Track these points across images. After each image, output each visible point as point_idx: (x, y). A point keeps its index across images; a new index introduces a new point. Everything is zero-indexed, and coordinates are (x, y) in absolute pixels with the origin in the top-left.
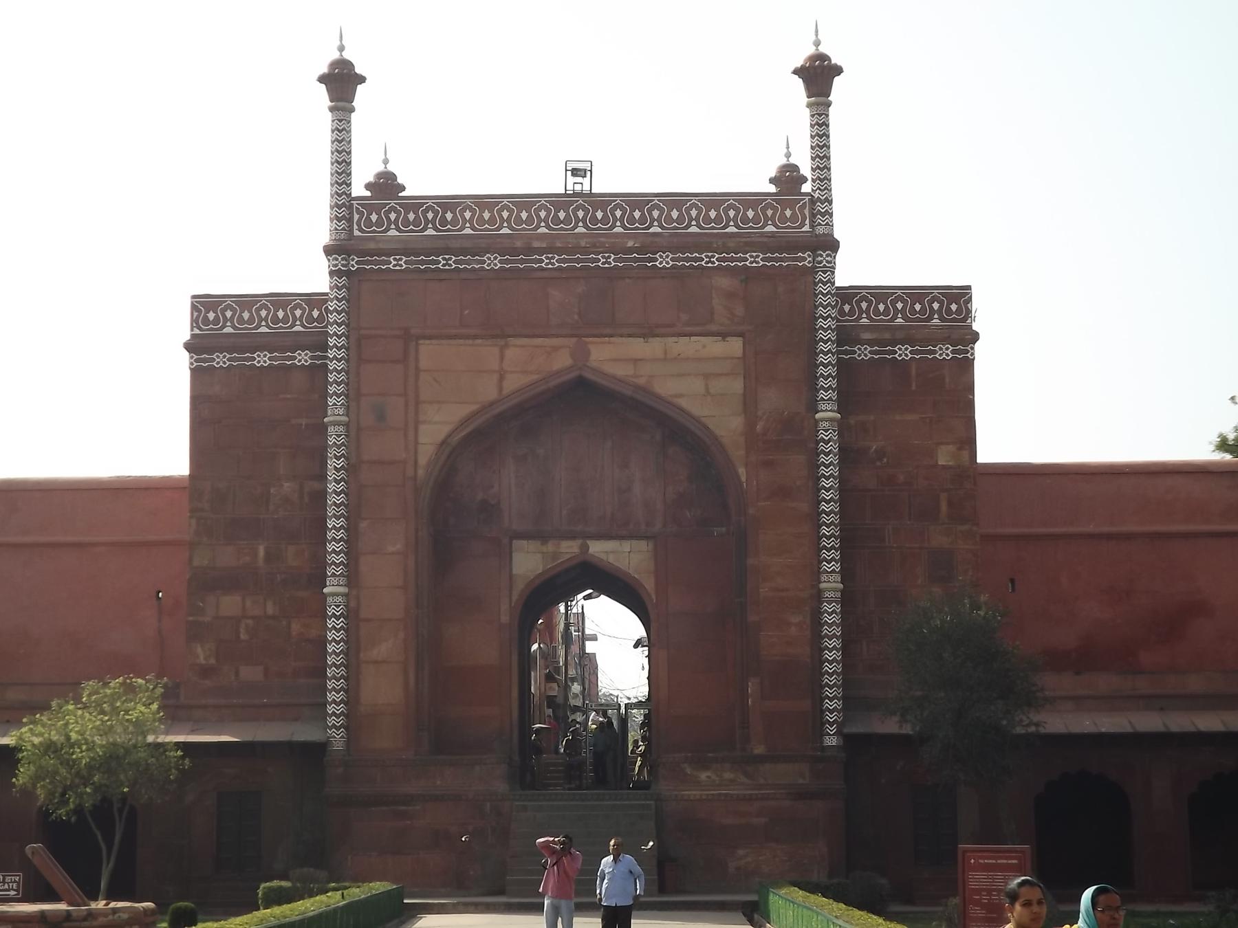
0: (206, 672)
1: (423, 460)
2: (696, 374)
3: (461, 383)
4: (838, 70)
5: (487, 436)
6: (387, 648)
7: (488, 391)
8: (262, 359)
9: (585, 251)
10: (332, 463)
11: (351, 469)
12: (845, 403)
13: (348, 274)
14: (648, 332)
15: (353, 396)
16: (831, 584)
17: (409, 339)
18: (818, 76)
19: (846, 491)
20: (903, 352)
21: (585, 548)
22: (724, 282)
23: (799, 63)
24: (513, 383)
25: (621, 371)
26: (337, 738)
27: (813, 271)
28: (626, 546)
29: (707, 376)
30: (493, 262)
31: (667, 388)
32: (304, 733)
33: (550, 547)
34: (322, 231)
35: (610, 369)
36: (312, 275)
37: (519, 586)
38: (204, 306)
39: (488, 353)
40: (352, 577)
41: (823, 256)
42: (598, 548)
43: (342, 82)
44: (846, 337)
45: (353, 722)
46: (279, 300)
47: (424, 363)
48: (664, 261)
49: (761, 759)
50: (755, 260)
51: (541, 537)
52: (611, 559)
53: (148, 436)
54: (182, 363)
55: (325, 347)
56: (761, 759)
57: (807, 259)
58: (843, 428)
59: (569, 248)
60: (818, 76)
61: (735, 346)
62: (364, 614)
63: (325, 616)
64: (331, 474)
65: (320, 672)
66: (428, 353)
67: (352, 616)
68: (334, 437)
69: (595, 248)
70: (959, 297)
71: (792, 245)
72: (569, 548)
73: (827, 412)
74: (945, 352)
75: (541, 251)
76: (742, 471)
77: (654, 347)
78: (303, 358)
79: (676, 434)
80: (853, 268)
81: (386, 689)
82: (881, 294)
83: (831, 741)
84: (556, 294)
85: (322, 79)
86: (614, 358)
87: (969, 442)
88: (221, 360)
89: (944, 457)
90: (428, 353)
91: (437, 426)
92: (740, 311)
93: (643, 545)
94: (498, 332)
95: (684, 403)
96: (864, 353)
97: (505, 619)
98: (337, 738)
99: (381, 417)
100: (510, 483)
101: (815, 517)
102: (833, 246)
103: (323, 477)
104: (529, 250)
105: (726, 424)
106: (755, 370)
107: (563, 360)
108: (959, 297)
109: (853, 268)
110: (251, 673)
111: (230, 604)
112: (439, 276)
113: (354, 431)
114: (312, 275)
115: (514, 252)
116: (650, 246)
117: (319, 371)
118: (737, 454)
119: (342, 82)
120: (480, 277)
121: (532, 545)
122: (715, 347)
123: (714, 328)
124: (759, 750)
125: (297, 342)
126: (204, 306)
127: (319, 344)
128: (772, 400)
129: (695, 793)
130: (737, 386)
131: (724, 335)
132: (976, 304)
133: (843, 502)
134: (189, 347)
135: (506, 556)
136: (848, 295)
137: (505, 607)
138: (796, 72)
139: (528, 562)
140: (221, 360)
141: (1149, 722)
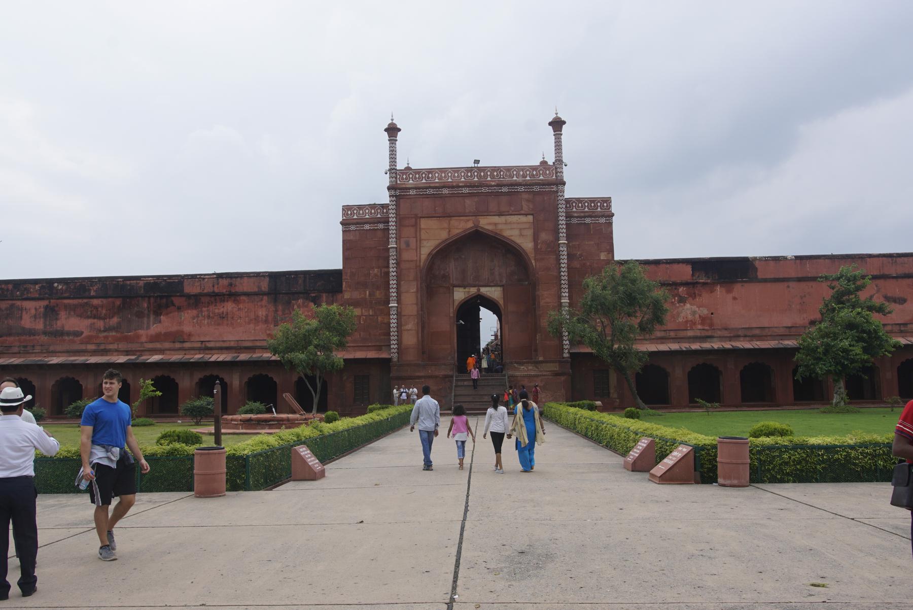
1: (422, 261)
2: (516, 229)
4: (564, 123)
5: (445, 252)
6: (411, 326)
7: (444, 235)
8: (367, 227)
9: (477, 187)
10: (391, 262)
11: (398, 264)
12: (568, 238)
13: (396, 196)
14: (500, 214)
16: (565, 301)
17: (417, 218)
18: (557, 124)
19: (569, 268)
20: (588, 221)
21: (479, 290)
22: (525, 196)
23: (551, 120)
25: (490, 228)
26: (395, 357)
27: (557, 192)
28: (493, 289)
29: (521, 229)
30: (446, 191)
31: (507, 233)
32: (384, 355)
33: (467, 290)
34: (386, 181)
35: (487, 227)
37: (456, 303)
38: (346, 209)
40: (399, 301)
41: (560, 187)
42: (484, 290)
43: (393, 131)
44: (569, 216)
45: (400, 351)
46: (373, 206)
47: (423, 226)
49: (542, 362)
50: (536, 189)
51: (465, 287)
52: (488, 294)
53: (327, 255)
55: (388, 222)
56: (542, 362)
57: (555, 189)
58: (568, 246)
59: (472, 186)
60: (557, 124)
61: (530, 218)
62: (403, 313)
63: (390, 315)
64: (391, 266)
66: (424, 223)
67: (399, 314)
68: (392, 253)
70: (607, 201)
71: (550, 184)
72: (473, 290)
73: (563, 241)
75: (462, 187)
76: (533, 261)
77: (502, 219)
78: (381, 226)
80: (571, 191)
81: (410, 339)
82: (579, 200)
83: (566, 355)
84: (468, 202)
85: (386, 130)
86: (487, 223)
87: (611, 251)
89: (603, 256)
90: (424, 223)
92: (531, 206)
93: (499, 289)
94: (448, 216)
95: (512, 238)
96: (575, 221)
97: (452, 315)
98: (395, 357)
99: (408, 245)
100: (452, 268)
101: (559, 278)
102: (564, 184)
103: (388, 267)
104: (458, 187)
105: (527, 245)
107: (470, 225)
108: (607, 201)
109: (571, 191)
112: (427, 196)
113: (399, 251)
115: (453, 187)
118: (532, 255)
119: (393, 131)
120: (442, 197)
121: (461, 289)
122: (523, 219)
123: (522, 212)
124: (541, 359)
125: (379, 221)
126: (346, 209)
127: (387, 222)
128: (544, 236)
129: (517, 374)
131: (526, 215)
132: (613, 204)
133: (568, 272)
134: (341, 223)
135: (452, 293)
136: (568, 201)
137: (451, 310)
138: (550, 124)
139: (460, 295)
141: (674, 347)
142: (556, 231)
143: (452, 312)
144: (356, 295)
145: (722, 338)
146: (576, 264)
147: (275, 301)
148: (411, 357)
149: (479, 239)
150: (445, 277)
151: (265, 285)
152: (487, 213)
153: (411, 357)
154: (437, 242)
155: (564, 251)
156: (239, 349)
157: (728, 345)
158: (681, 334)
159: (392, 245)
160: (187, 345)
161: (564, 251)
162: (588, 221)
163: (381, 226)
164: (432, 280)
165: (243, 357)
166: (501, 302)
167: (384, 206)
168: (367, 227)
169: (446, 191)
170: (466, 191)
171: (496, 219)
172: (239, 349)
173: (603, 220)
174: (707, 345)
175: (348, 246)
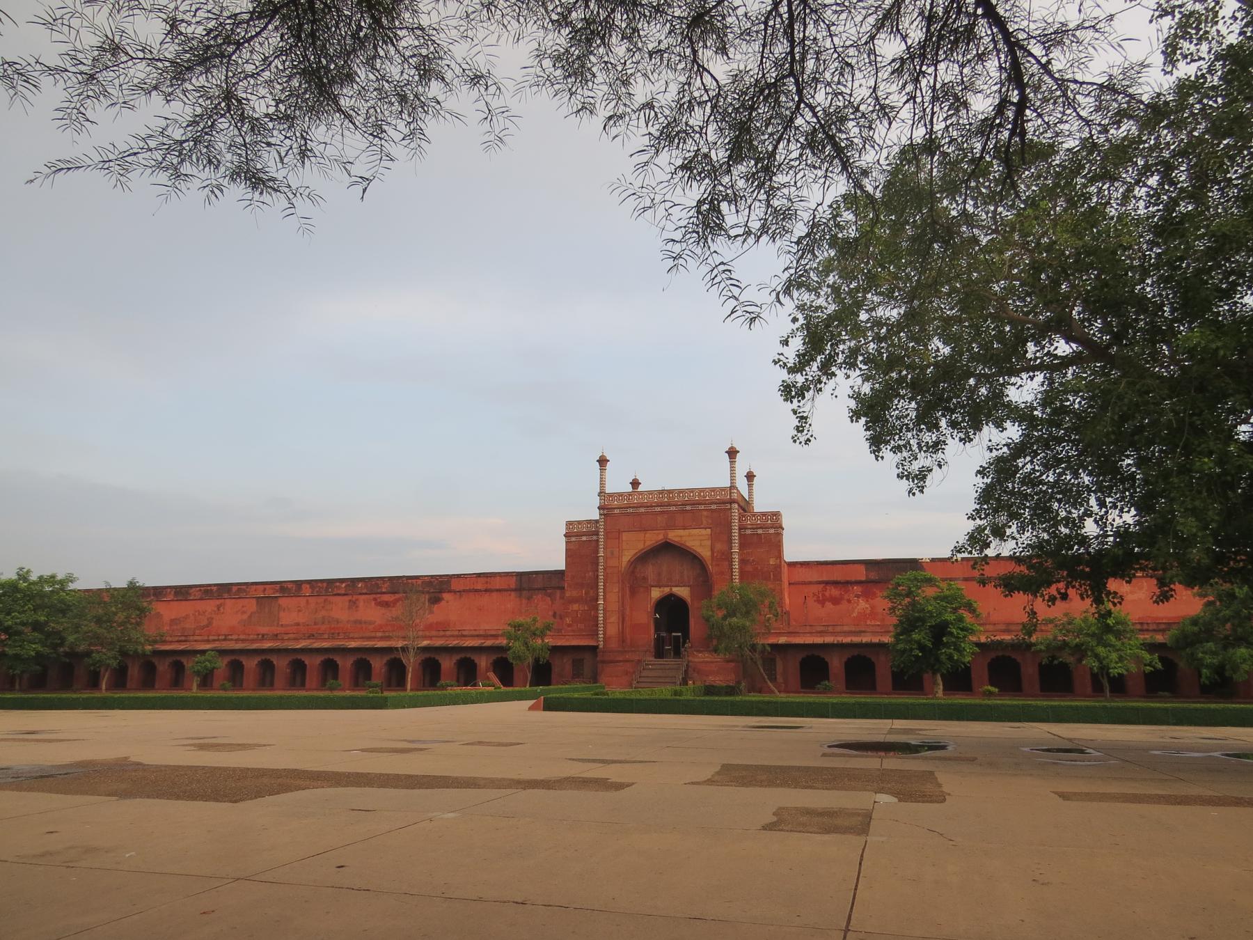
0: (569, 625)
2: (698, 540)
5: (645, 557)
6: (614, 619)
7: (641, 546)
8: (584, 538)
14: (685, 528)
17: (619, 532)
20: (760, 531)
22: (705, 513)
30: (642, 510)
36: (595, 515)
38: (569, 524)
39: (642, 534)
43: (603, 461)
48: (688, 508)
50: (713, 507)
58: (740, 554)
68: (601, 560)
69: (669, 505)
70: (777, 515)
71: (724, 503)
72: (667, 590)
74: (772, 531)
78: (595, 538)
81: (613, 630)
86: (675, 536)
91: (627, 557)
96: (748, 532)
100: (650, 571)
105: (705, 553)
106: (714, 538)
108: (777, 515)
110: (581, 626)
111: (576, 607)
113: (606, 558)
114: (595, 515)
118: (709, 563)
119: (603, 461)
122: (703, 532)
126: (569, 524)
128: (719, 546)
130: (709, 543)
139: (656, 594)
142: (730, 541)
143: (650, 607)
144: (575, 593)
145: (874, 633)
146: (749, 568)
147: (520, 596)
148: (614, 645)
149: (667, 548)
150: (645, 579)
151: (513, 583)
152: (674, 527)
153: (614, 645)
154: (633, 552)
155: (736, 557)
156: (486, 637)
157: (875, 640)
158: (838, 629)
159: (601, 554)
160: (448, 633)
161: (736, 557)
162: (760, 531)
164: (633, 581)
165: (489, 643)
166: (689, 600)
167: (597, 521)
168: (584, 538)
169: (642, 510)
171: (681, 532)
172: (486, 637)
173: (772, 531)
174: (856, 639)
175: (570, 554)
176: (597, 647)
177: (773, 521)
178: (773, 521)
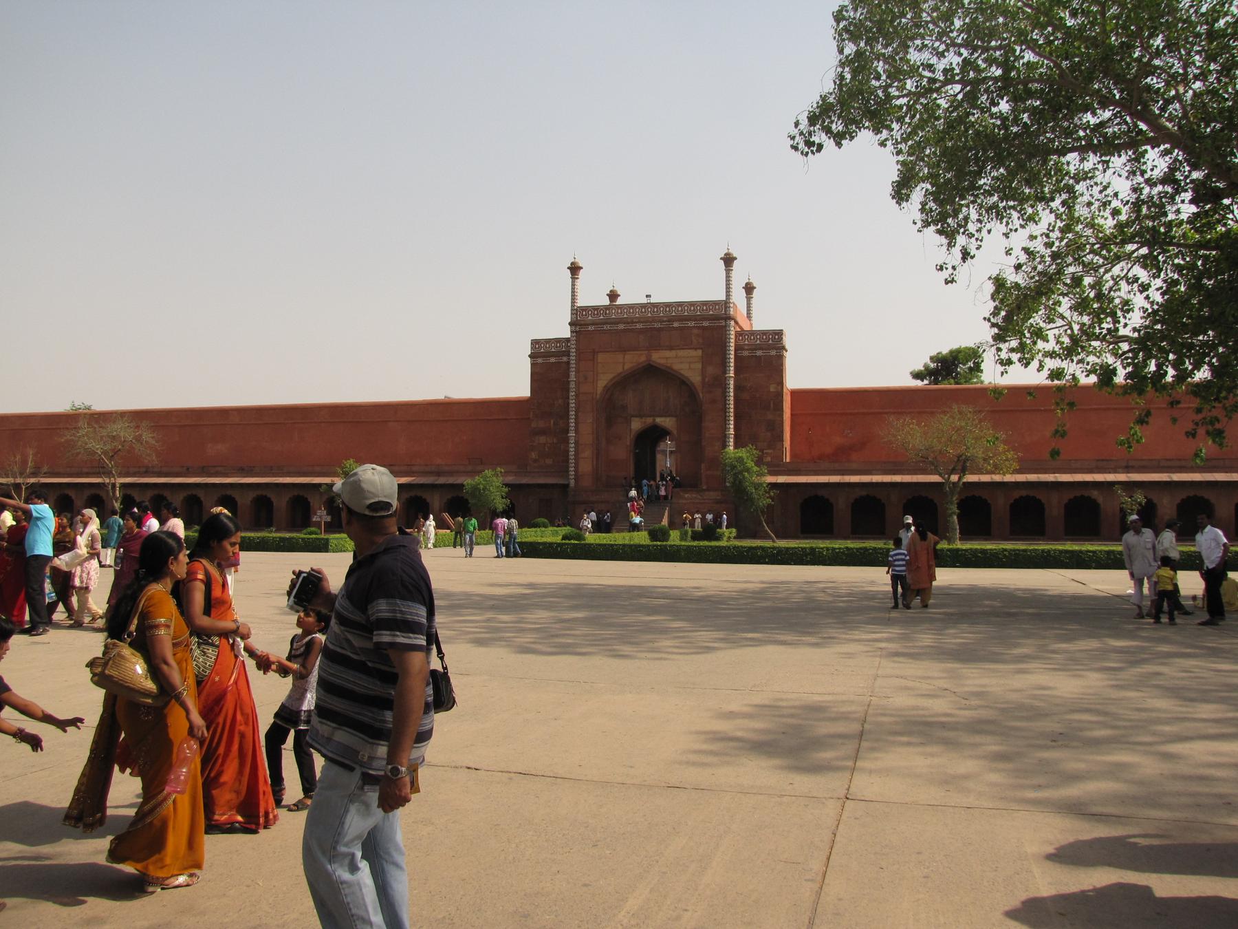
0: (535, 461)
2: (686, 363)
3: (611, 367)
5: (624, 382)
6: (587, 453)
8: (553, 360)
14: (671, 348)
15: (577, 371)
17: (594, 353)
20: (759, 353)
22: (695, 331)
24: (626, 367)
28: (668, 419)
30: (621, 327)
31: (676, 367)
36: (566, 333)
38: (535, 343)
40: (577, 431)
42: (659, 420)
43: (575, 269)
48: (676, 325)
50: (706, 324)
54: (527, 363)
61: (700, 352)
65: (567, 461)
67: (576, 443)
68: (572, 385)
70: (779, 334)
72: (649, 420)
74: (773, 353)
78: (565, 359)
79: (682, 383)
81: (586, 467)
86: (660, 357)
88: (540, 360)
91: (603, 382)
96: (746, 353)
98: (572, 483)
105: (695, 378)
106: (705, 361)
108: (779, 334)
111: (542, 439)
113: (578, 383)
114: (566, 333)
116: (671, 320)
117: (568, 363)
119: (575, 269)
122: (692, 353)
126: (535, 343)
127: (567, 354)
128: (711, 370)
130: (699, 366)
139: (636, 425)
140: (540, 360)
143: (628, 440)
144: (541, 424)
149: (651, 371)
152: (658, 347)
163: (565, 359)
164: (610, 409)
165: (442, 480)
167: (568, 340)
168: (553, 360)
170: (639, 326)
171: (668, 354)
173: (773, 353)
176: (567, 486)
177: (773, 343)
178: (773, 343)
